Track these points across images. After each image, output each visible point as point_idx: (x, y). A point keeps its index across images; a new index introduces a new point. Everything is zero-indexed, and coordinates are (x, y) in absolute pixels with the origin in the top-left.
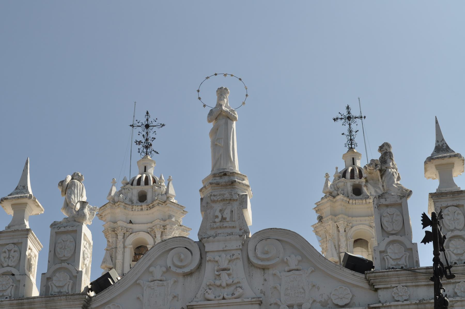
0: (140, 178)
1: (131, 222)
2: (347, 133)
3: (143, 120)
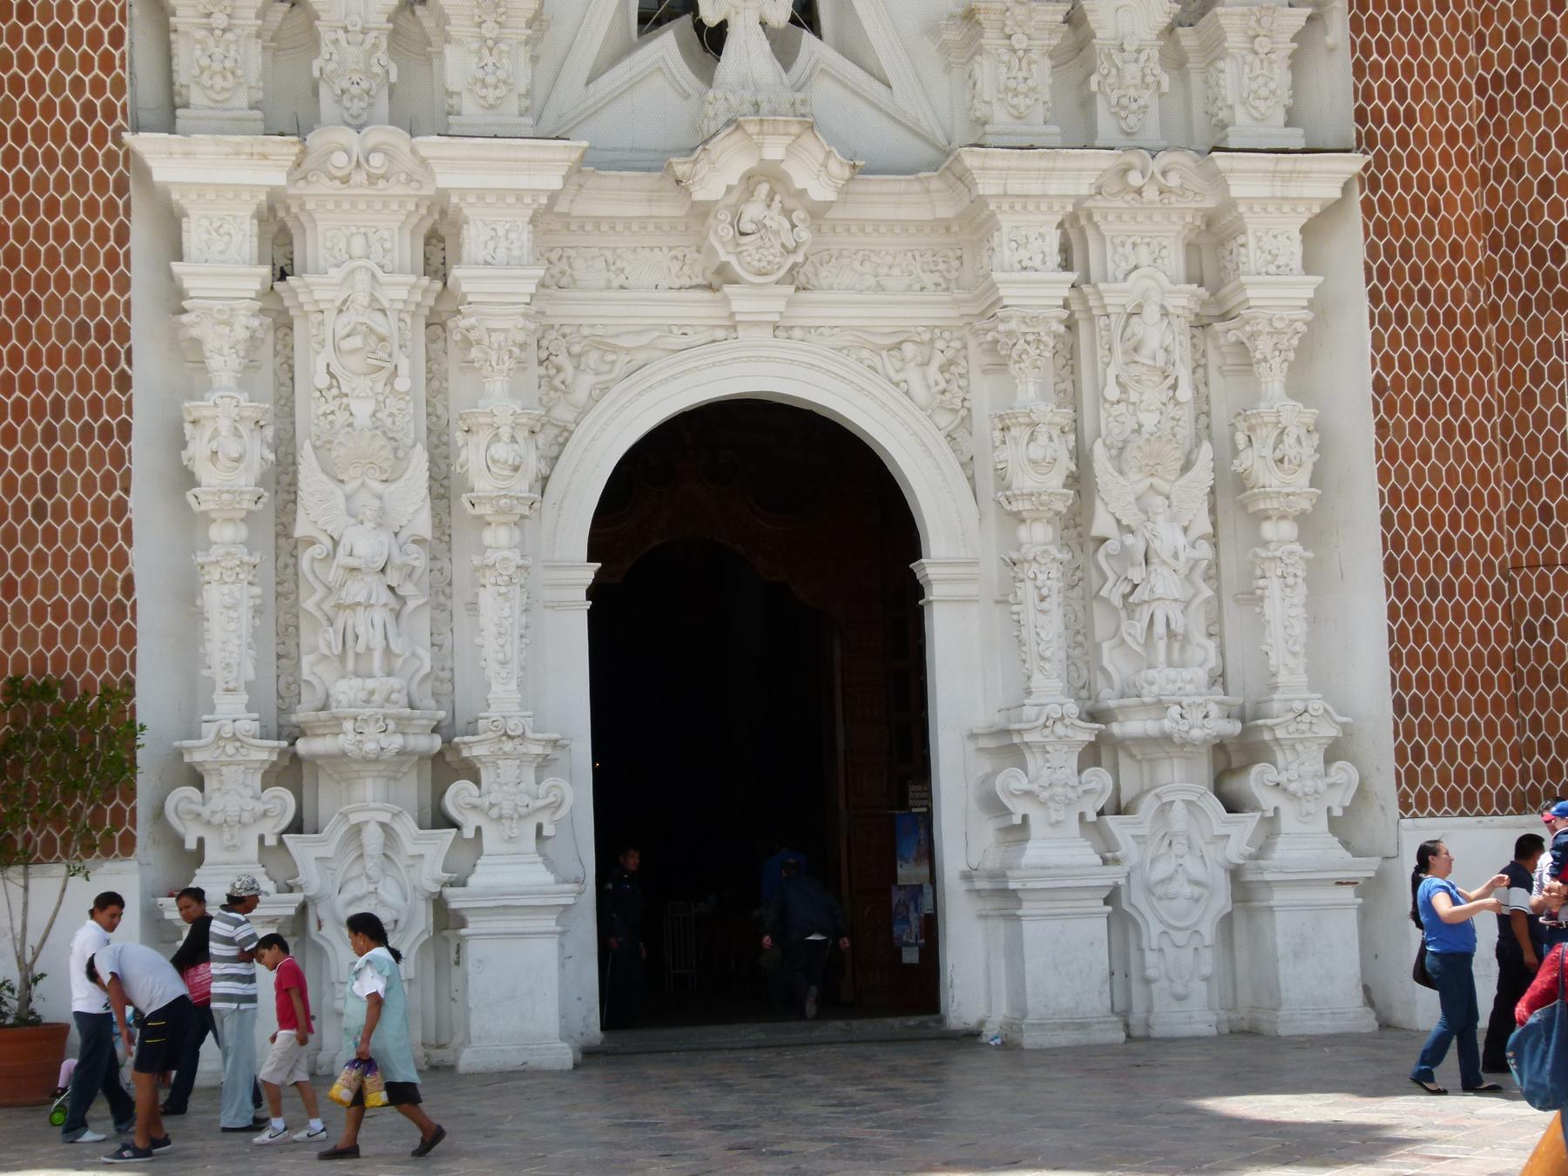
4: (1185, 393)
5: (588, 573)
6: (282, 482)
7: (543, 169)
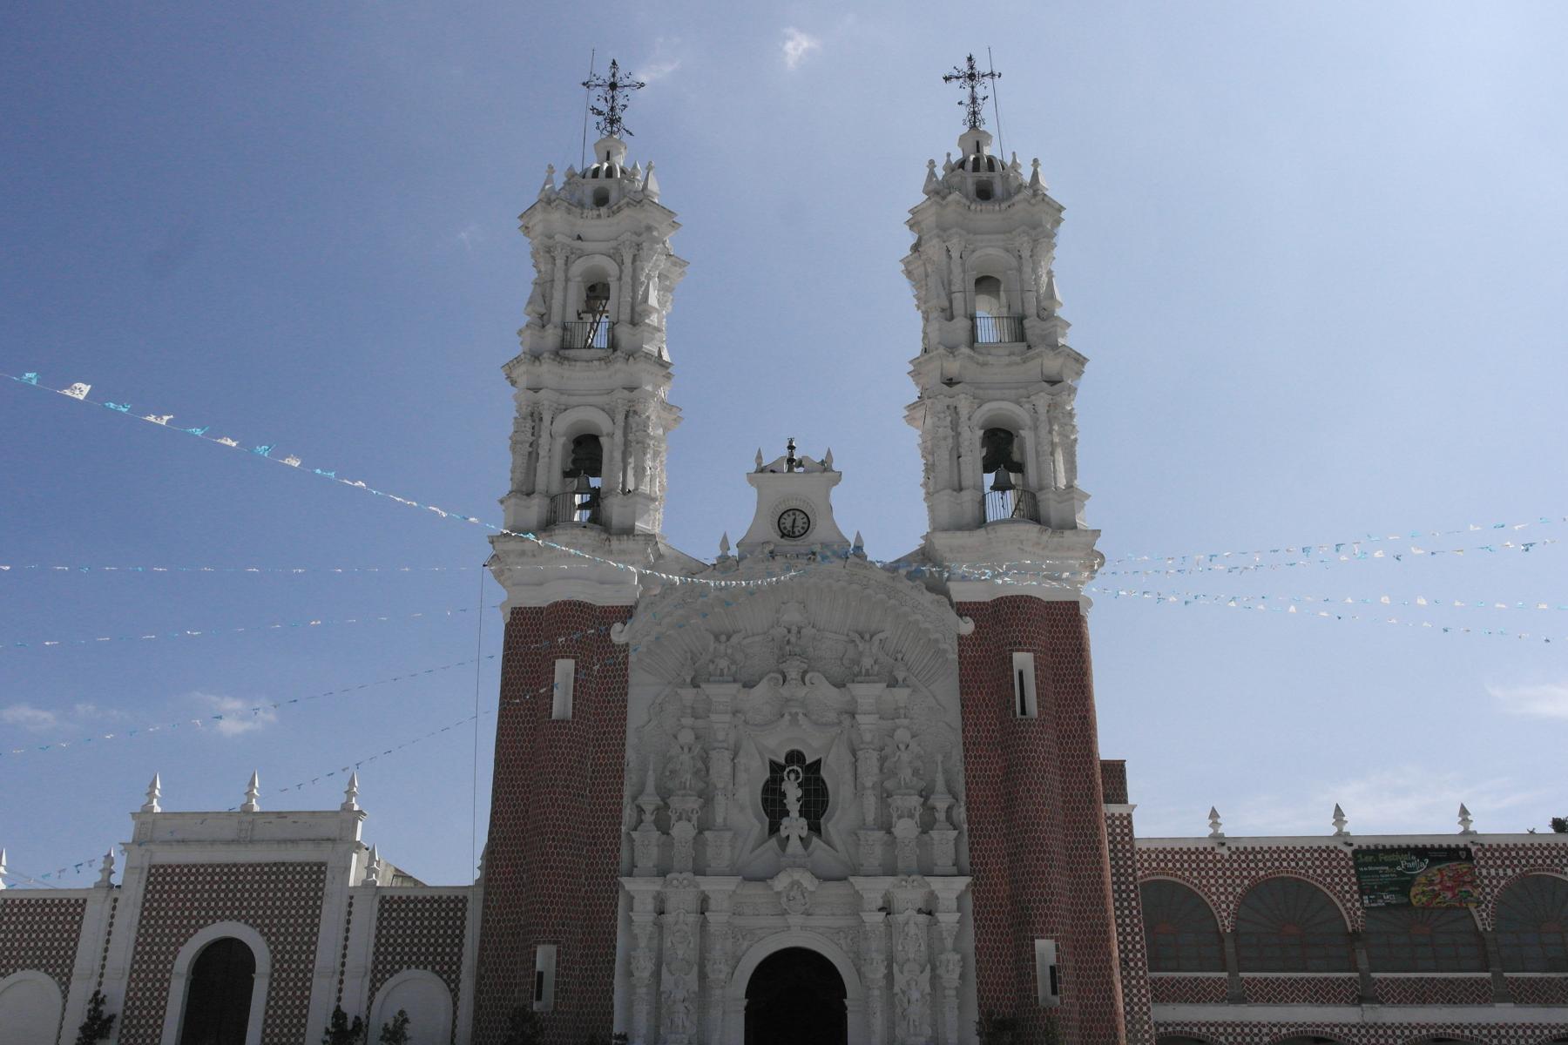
0: (597, 170)
1: (579, 238)
2: (967, 101)
3: (606, 75)
4: (923, 948)
5: (745, 1002)
6: (657, 974)
7: (730, 884)
